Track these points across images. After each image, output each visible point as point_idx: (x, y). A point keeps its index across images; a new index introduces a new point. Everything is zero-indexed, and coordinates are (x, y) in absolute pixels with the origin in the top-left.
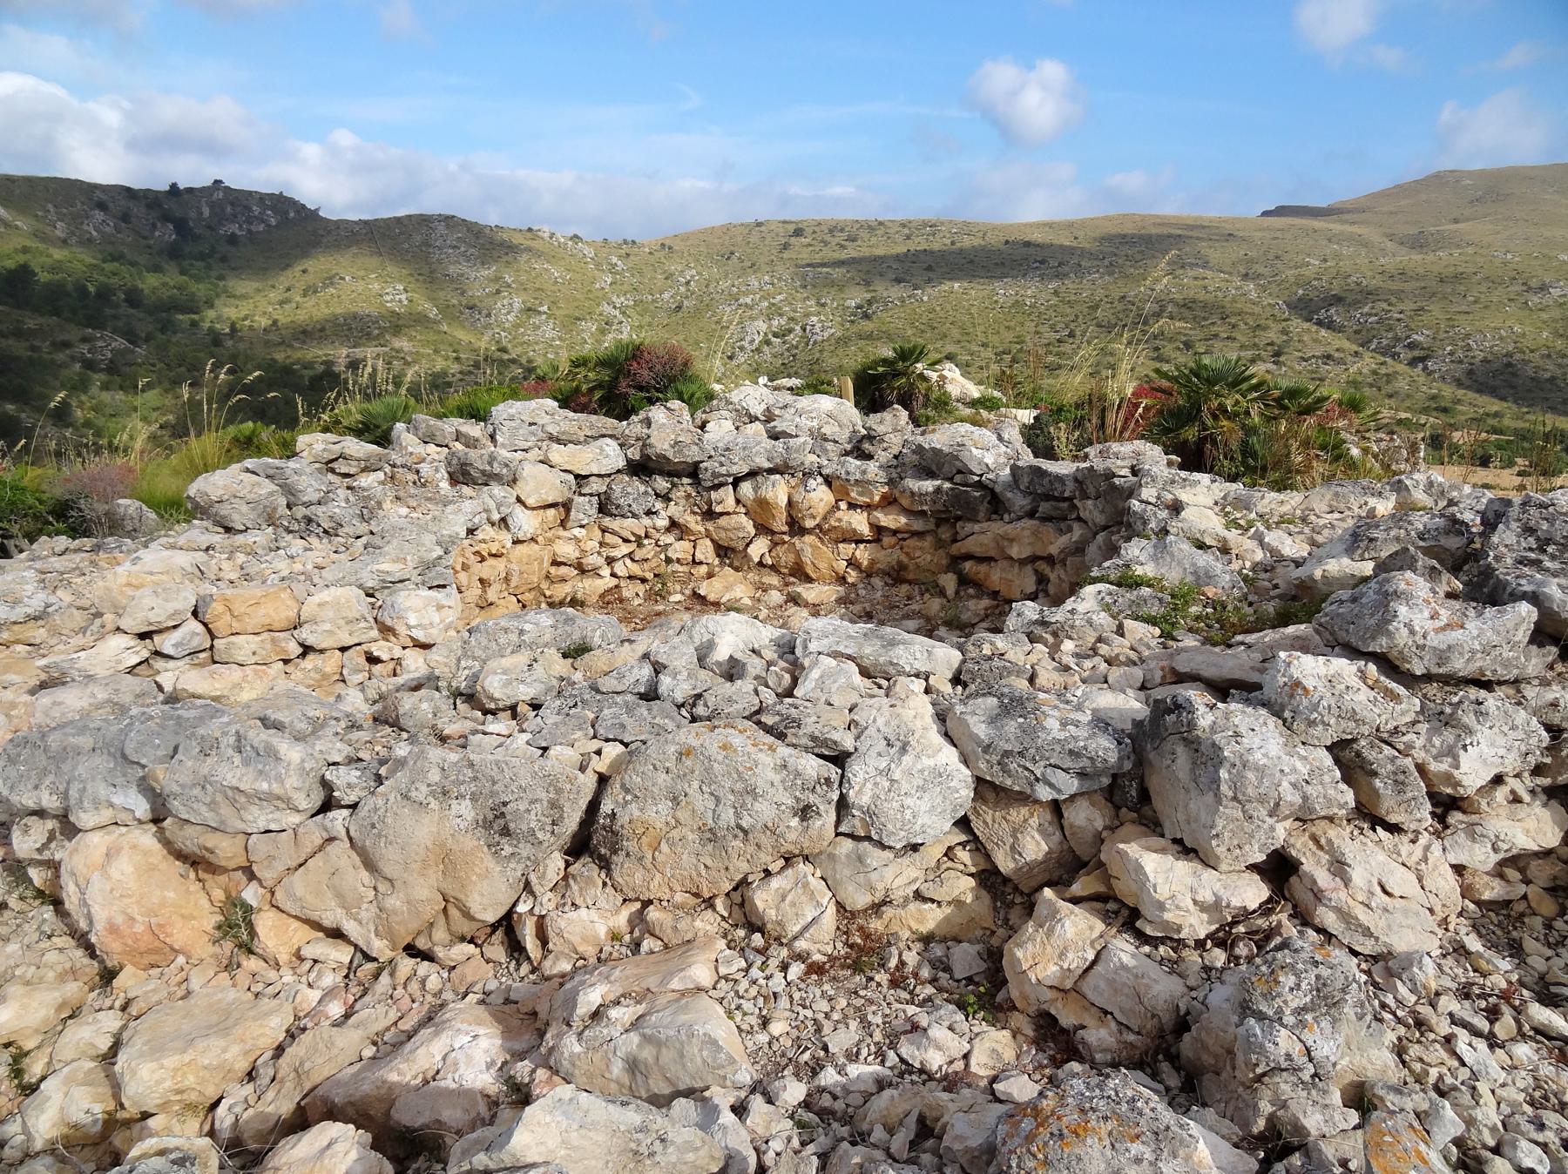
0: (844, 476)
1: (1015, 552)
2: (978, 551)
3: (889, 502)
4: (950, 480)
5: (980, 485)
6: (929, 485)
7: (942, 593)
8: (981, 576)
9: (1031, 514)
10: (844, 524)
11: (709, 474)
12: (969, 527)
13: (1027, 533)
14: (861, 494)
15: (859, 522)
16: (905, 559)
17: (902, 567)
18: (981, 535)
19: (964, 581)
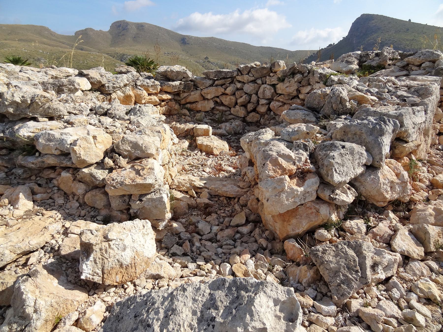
0: (146, 84)
1: (209, 97)
2: (193, 100)
3: (161, 91)
4: (181, 80)
5: (191, 81)
6: (177, 83)
7: (185, 115)
8: (194, 107)
9: (211, 85)
10: (153, 100)
11: (111, 88)
12: (186, 95)
13: (214, 90)
14: (153, 90)
15: (155, 98)
16: (169, 108)
17: (170, 111)
18: (194, 95)
19: (189, 110)
